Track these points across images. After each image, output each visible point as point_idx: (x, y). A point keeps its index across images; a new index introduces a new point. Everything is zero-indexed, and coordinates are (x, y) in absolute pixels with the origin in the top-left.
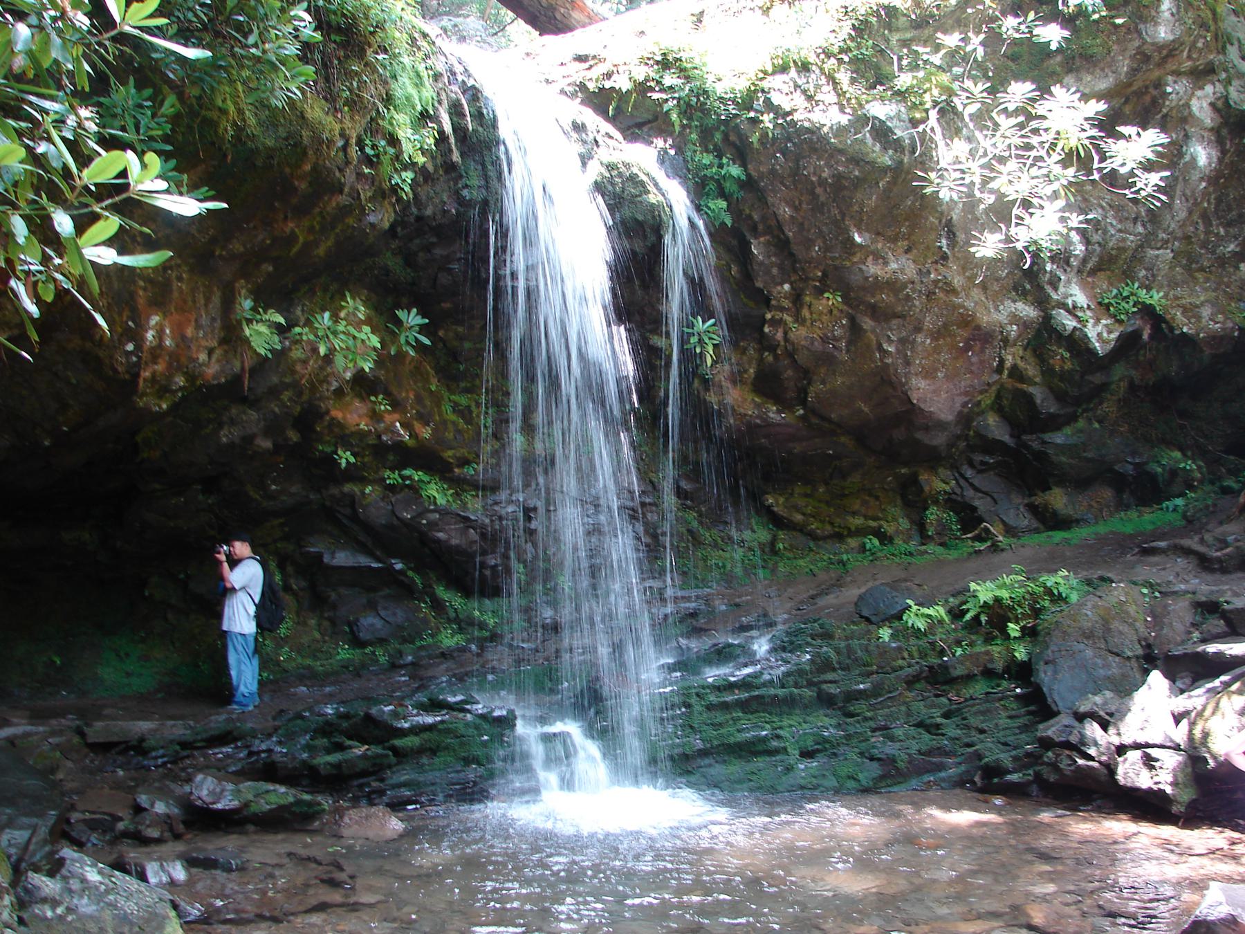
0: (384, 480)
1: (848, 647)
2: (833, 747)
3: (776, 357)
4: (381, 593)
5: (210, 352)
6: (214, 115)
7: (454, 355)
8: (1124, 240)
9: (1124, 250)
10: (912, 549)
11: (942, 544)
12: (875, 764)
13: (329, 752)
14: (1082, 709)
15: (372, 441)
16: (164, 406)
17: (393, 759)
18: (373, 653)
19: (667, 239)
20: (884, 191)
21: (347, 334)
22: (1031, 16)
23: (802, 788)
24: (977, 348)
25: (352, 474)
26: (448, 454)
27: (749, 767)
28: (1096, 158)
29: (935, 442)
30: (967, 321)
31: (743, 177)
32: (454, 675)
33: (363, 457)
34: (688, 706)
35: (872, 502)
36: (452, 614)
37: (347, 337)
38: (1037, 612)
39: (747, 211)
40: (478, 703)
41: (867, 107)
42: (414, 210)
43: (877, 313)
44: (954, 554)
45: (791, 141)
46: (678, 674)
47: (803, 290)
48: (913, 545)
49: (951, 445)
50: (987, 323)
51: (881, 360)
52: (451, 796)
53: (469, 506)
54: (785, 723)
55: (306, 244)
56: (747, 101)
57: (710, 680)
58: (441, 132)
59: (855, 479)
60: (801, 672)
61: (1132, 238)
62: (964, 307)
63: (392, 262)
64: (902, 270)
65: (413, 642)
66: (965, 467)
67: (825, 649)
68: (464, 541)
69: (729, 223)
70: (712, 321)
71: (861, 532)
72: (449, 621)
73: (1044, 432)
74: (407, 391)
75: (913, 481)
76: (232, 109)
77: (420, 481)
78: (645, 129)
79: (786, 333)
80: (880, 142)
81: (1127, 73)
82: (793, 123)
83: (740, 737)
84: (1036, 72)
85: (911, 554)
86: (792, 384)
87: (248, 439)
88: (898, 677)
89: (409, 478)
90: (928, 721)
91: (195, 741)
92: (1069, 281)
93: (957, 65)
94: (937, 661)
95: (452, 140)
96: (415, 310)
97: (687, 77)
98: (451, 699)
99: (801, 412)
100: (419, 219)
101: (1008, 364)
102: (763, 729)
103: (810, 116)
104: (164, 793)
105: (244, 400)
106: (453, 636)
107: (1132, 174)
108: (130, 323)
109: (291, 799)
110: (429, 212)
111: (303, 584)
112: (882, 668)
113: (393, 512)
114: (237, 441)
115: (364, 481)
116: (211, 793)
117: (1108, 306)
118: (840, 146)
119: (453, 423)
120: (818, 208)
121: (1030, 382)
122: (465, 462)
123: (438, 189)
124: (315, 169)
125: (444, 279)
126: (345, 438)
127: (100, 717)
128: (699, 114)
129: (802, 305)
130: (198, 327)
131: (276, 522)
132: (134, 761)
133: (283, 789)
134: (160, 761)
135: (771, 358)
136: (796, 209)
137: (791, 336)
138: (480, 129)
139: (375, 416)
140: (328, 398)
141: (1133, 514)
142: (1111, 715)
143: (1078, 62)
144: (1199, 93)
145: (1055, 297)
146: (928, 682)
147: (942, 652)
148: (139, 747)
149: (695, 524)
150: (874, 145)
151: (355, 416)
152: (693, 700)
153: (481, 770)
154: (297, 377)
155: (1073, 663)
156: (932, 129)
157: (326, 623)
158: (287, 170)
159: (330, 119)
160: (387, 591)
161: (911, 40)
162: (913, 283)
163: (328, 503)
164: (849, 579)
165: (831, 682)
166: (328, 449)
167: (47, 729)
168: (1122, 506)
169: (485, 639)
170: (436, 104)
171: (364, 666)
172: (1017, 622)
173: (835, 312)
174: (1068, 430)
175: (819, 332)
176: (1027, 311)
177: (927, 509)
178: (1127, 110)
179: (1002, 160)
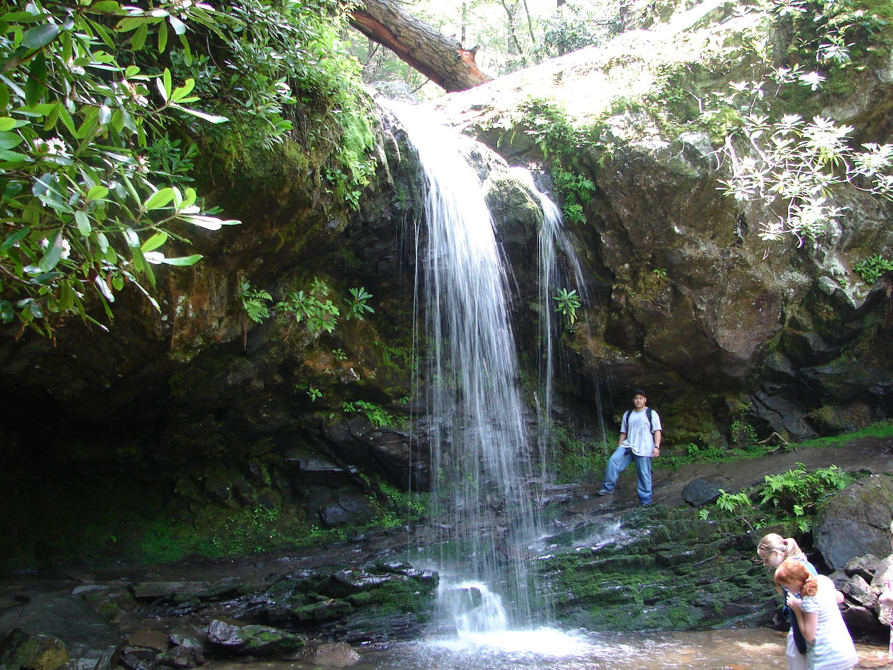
1: (677, 524)
2: (668, 597)
3: (620, 316)
5: (220, 320)
6: (222, 156)
7: (391, 320)
8: (870, 225)
9: (871, 232)
10: (722, 453)
11: (743, 448)
12: (699, 609)
13: (305, 604)
14: (851, 568)
15: (334, 381)
16: (189, 359)
17: (351, 609)
18: (336, 532)
20: (695, 195)
21: (317, 306)
22: (797, 67)
23: (646, 627)
25: (320, 405)
26: (388, 390)
27: (608, 612)
28: (848, 167)
29: (736, 375)
30: (757, 286)
31: (594, 189)
32: (394, 548)
33: (328, 393)
34: (563, 569)
35: (692, 418)
36: (392, 504)
37: (316, 308)
38: (815, 497)
39: (597, 213)
40: (411, 568)
42: (361, 218)
43: (691, 282)
44: (753, 455)
45: (627, 162)
46: (555, 545)
47: (638, 267)
48: (722, 449)
49: (748, 377)
51: (696, 316)
52: (392, 635)
54: (632, 580)
55: (286, 243)
56: (596, 133)
59: (680, 402)
60: (644, 543)
61: (876, 223)
63: (346, 255)
64: (709, 252)
65: (365, 525)
66: (759, 392)
69: (584, 221)
70: (574, 291)
71: (684, 441)
72: (390, 509)
73: (816, 365)
75: (722, 403)
76: (234, 151)
77: (369, 410)
79: (627, 299)
80: (691, 161)
81: (868, 105)
82: (629, 149)
83: (601, 591)
84: (802, 107)
85: (721, 456)
86: (632, 335)
87: (247, 382)
88: (714, 546)
89: (360, 407)
90: (737, 578)
91: (210, 596)
92: (831, 256)
93: (745, 104)
95: (387, 168)
97: (552, 119)
98: (393, 565)
99: (640, 355)
101: (788, 317)
102: (617, 584)
104: (191, 634)
105: (244, 354)
106: (393, 520)
107: (874, 177)
109: (279, 637)
110: (372, 219)
111: (286, 484)
112: (702, 539)
113: (349, 432)
115: (328, 410)
116: (223, 633)
117: (860, 273)
118: (662, 165)
119: (391, 368)
120: (647, 209)
121: (805, 329)
122: (401, 396)
123: (378, 202)
124: (291, 191)
125: (383, 266)
126: (315, 380)
127: (144, 579)
128: (561, 145)
129: (638, 279)
130: (212, 303)
131: (267, 440)
132: (169, 610)
133: (273, 630)
134: (186, 610)
135: (616, 317)
136: (632, 210)
137: (631, 301)
139: (336, 364)
140: (303, 352)
141: (884, 423)
142: (873, 572)
143: (832, 99)
145: (821, 267)
147: (746, 527)
148: (171, 601)
149: (564, 437)
150: (686, 163)
151: (322, 364)
152: (567, 564)
153: (415, 616)
154: (281, 337)
155: (843, 533)
156: (728, 150)
157: (302, 512)
158: (273, 192)
159: (302, 156)
160: (346, 488)
161: (711, 87)
162: (717, 260)
164: (676, 475)
165: (666, 550)
166: (303, 388)
168: (875, 418)
169: (415, 522)
171: (329, 542)
172: (800, 504)
173: (662, 283)
174: (834, 363)
176: (801, 278)
177: (732, 423)
178: (869, 131)
179: (779, 171)
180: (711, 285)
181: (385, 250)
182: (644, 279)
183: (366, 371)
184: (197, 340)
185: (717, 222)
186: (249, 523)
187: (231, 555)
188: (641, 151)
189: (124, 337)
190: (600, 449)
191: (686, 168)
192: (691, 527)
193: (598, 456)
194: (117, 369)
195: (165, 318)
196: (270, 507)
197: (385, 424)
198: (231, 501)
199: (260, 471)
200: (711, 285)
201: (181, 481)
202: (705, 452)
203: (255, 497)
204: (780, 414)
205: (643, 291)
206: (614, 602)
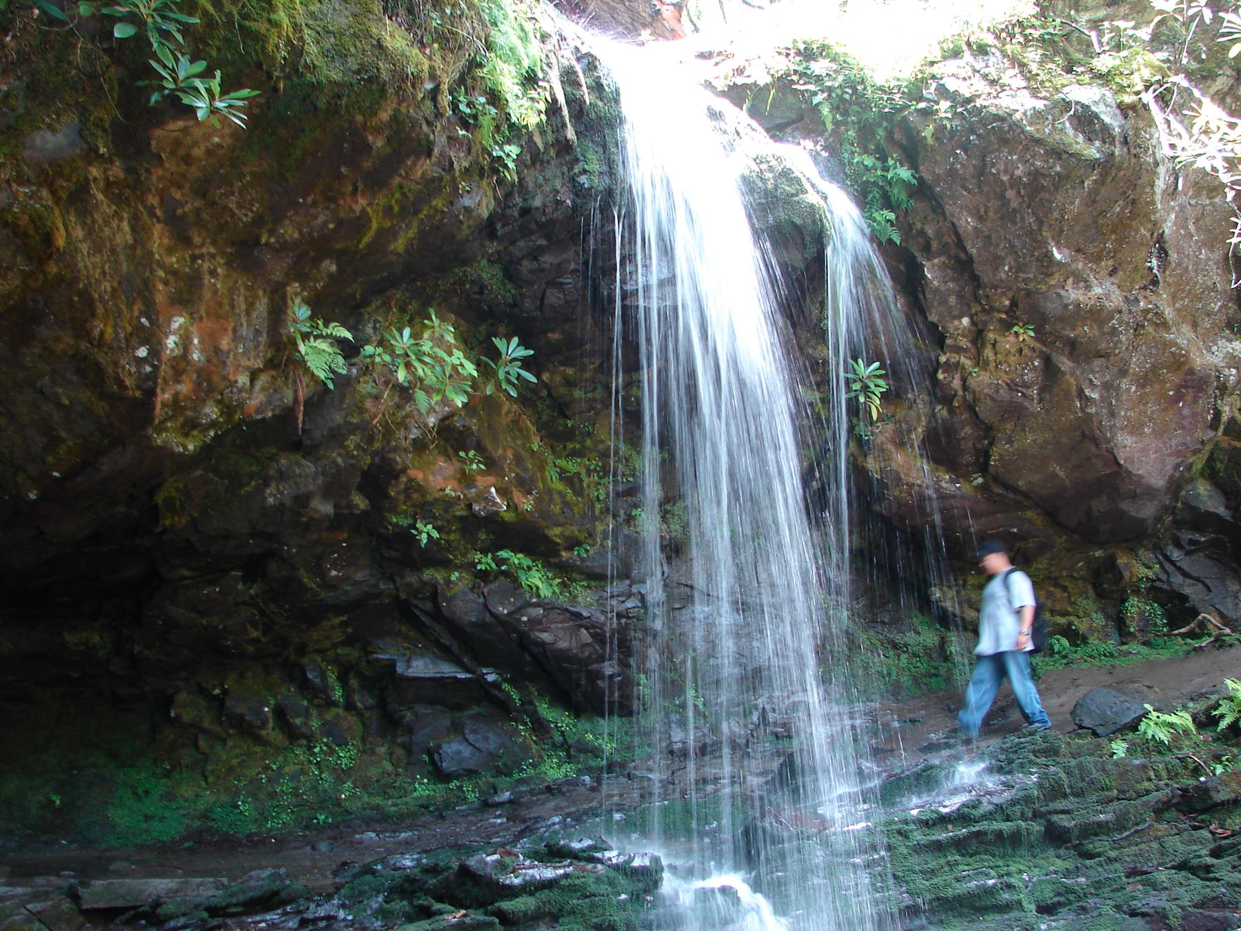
0: (474, 565)
1: (1080, 766)
2: (1079, 899)
3: (952, 411)
4: (470, 712)
5: (254, 376)
6: (262, 27)
7: (562, 408)
10: (1113, 650)
11: (1145, 643)
15: (460, 512)
16: (191, 447)
18: (460, 788)
19: (829, 251)
20: (1090, 193)
21: (435, 358)
24: (1189, 398)
25: (435, 556)
26: (555, 532)
29: (1141, 515)
30: (1179, 362)
31: (914, 182)
32: (568, 815)
33: (449, 532)
35: (1058, 593)
36: (558, 738)
37: (432, 363)
39: (919, 226)
40: (610, 849)
41: (1065, 90)
42: (518, 200)
43: (1073, 348)
44: (1165, 655)
45: (973, 132)
47: (986, 323)
48: (1111, 644)
49: (1158, 519)
50: (1201, 365)
51: (1082, 409)
53: (580, 599)
54: (1013, 868)
55: (381, 232)
56: (915, 91)
57: (914, 812)
58: (555, 100)
60: (1027, 800)
62: (1176, 344)
63: (488, 273)
64: (1107, 296)
65: (509, 775)
66: (1170, 548)
67: (1052, 769)
68: (574, 644)
69: (897, 239)
70: (877, 364)
72: (555, 747)
74: (505, 450)
76: (286, 22)
77: (520, 567)
78: (789, 130)
79: (964, 380)
80: (1083, 132)
82: (979, 111)
83: (962, 888)
85: (1112, 656)
86: (970, 444)
87: (302, 500)
88: (1145, 804)
90: (1195, 862)
91: (228, 906)
94: (1192, 782)
95: (565, 112)
96: (515, 340)
98: (576, 845)
99: (980, 480)
100: (525, 212)
101: (1225, 418)
103: (997, 101)
106: (559, 767)
108: (143, 320)
110: (537, 202)
111: (371, 701)
112: (1124, 792)
113: (485, 605)
114: (288, 502)
115: (447, 565)
118: (1037, 136)
119: (560, 493)
120: (1008, 216)
122: (573, 543)
123: (548, 174)
124: (394, 118)
125: (554, 297)
126: (425, 510)
127: (104, 873)
128: (855, 108)
129: (983, 344)
130: (236, 338)
135: (945, 413)
136: (980, 218)
137: (972, 382)
138: (600, 103)
139: (466, 479)
146: (1178, 810)
147: (1197, 771)
150: (1076, 136)
151: (439, 477)
154: (367, 416)
157: (399, 752)
158: (359, 118)
159: (415, 51)
160: (477, 709)
162: (1120, 312)
163: (403, 596)
165: (1063, 812)
166: (404, 522)
167: (28, 890)
169: (601, 769)
170: (545, 67)
171: (447, 805)
173: (1026, 351)
175: (1005, 377)
177: (1124, 601)
180: (1105, 356)
181: (559, 265)
182: (994, 345)
183: (517, 495)
184: (207, 410)
185: (1121, 245)
186: (303, 772)
187: (271, 830)
188: (1001, 113)
189: (60, 390)
190: (906, 645)
191: (1077, 143)
192: (1104, 770)
193: (904, 657)
194: (50, 459)
195: (142, 352)
196: (342, 743)
197: (549, 594)
198: (271, 732)
199: (323, 677)
200: (1105, 356)
201: (182, 696)
202: (1081, 651)
203: (315, 724)
204: (1203, 583)
205: (992, 365)
206: (983, 910)
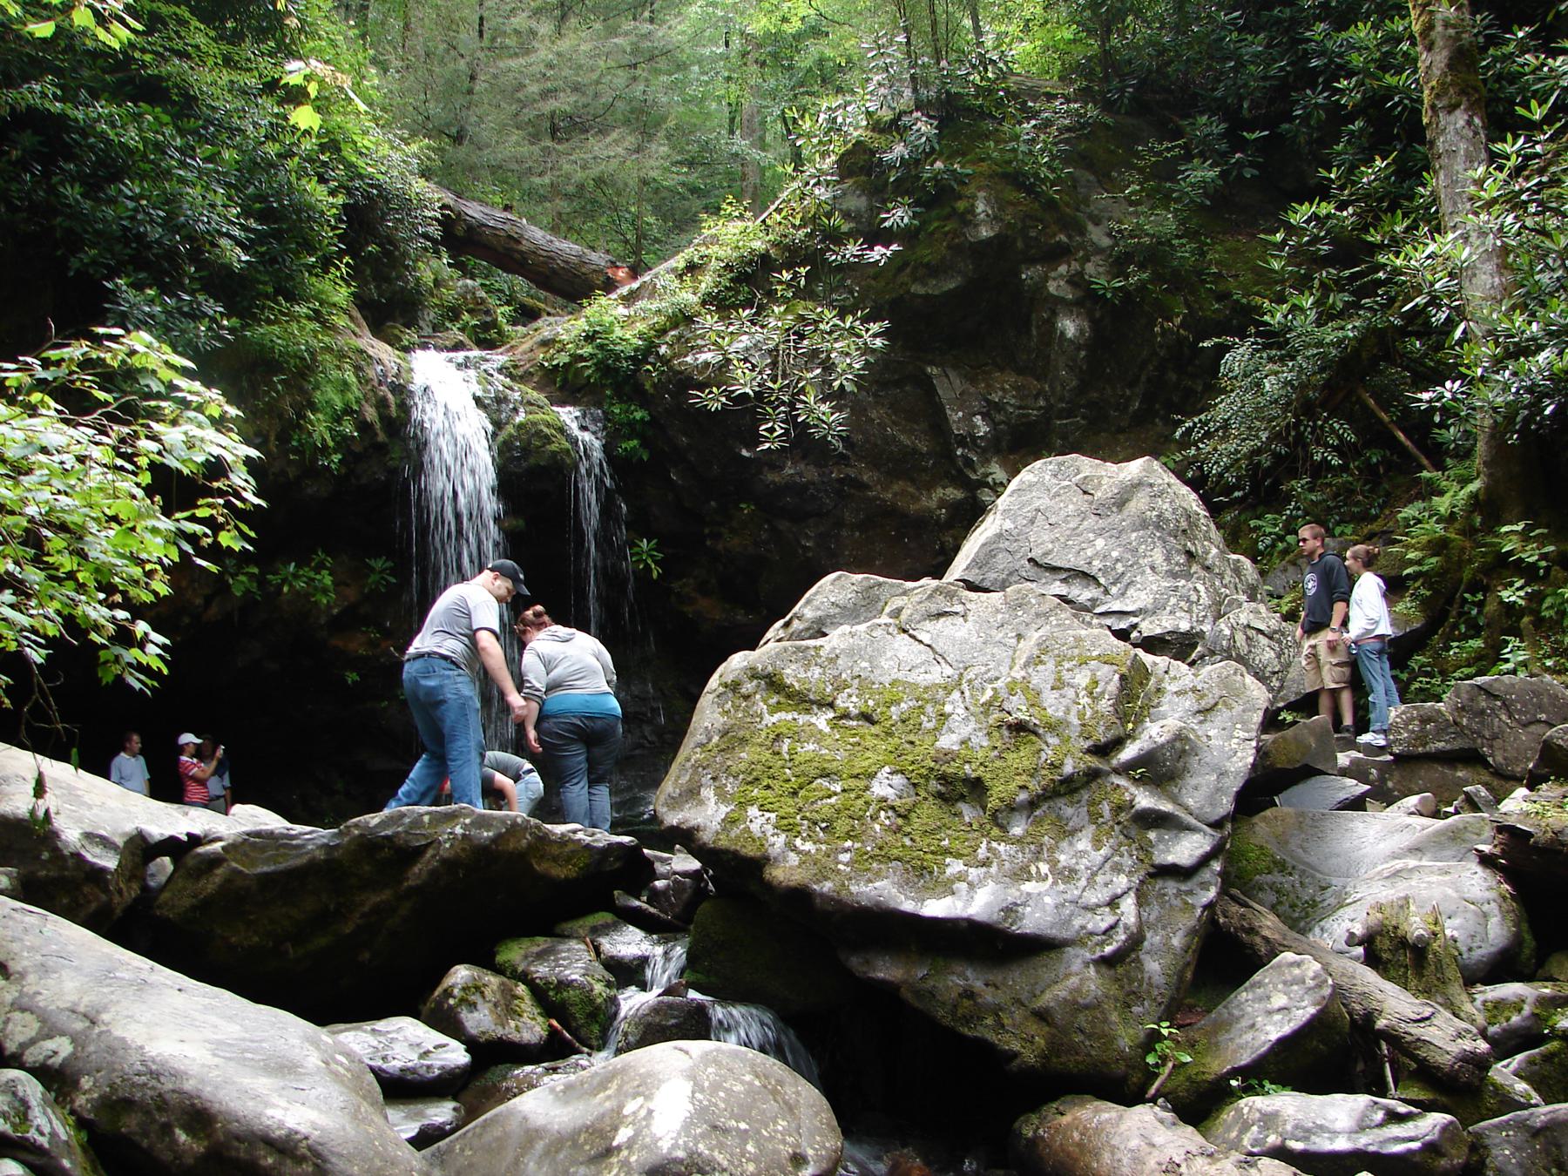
30: (890, 513)
31: (647, 418)
110: (364, 481)
144: (1053, 274)
